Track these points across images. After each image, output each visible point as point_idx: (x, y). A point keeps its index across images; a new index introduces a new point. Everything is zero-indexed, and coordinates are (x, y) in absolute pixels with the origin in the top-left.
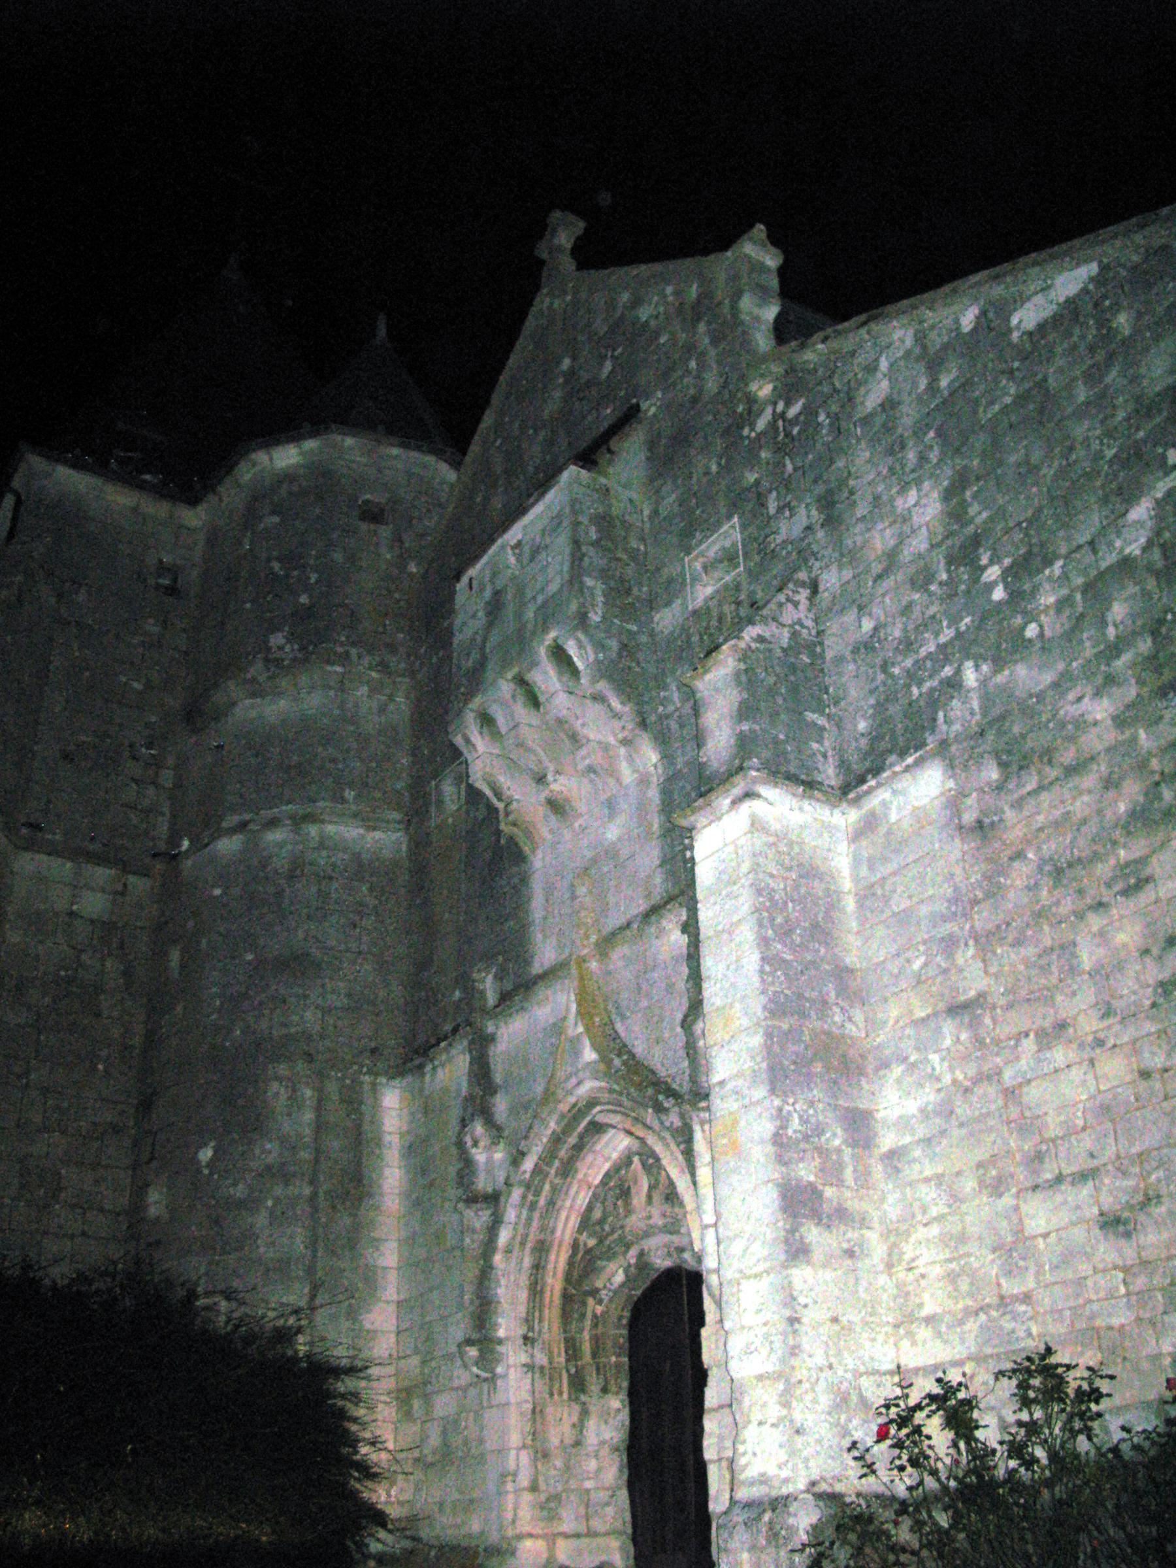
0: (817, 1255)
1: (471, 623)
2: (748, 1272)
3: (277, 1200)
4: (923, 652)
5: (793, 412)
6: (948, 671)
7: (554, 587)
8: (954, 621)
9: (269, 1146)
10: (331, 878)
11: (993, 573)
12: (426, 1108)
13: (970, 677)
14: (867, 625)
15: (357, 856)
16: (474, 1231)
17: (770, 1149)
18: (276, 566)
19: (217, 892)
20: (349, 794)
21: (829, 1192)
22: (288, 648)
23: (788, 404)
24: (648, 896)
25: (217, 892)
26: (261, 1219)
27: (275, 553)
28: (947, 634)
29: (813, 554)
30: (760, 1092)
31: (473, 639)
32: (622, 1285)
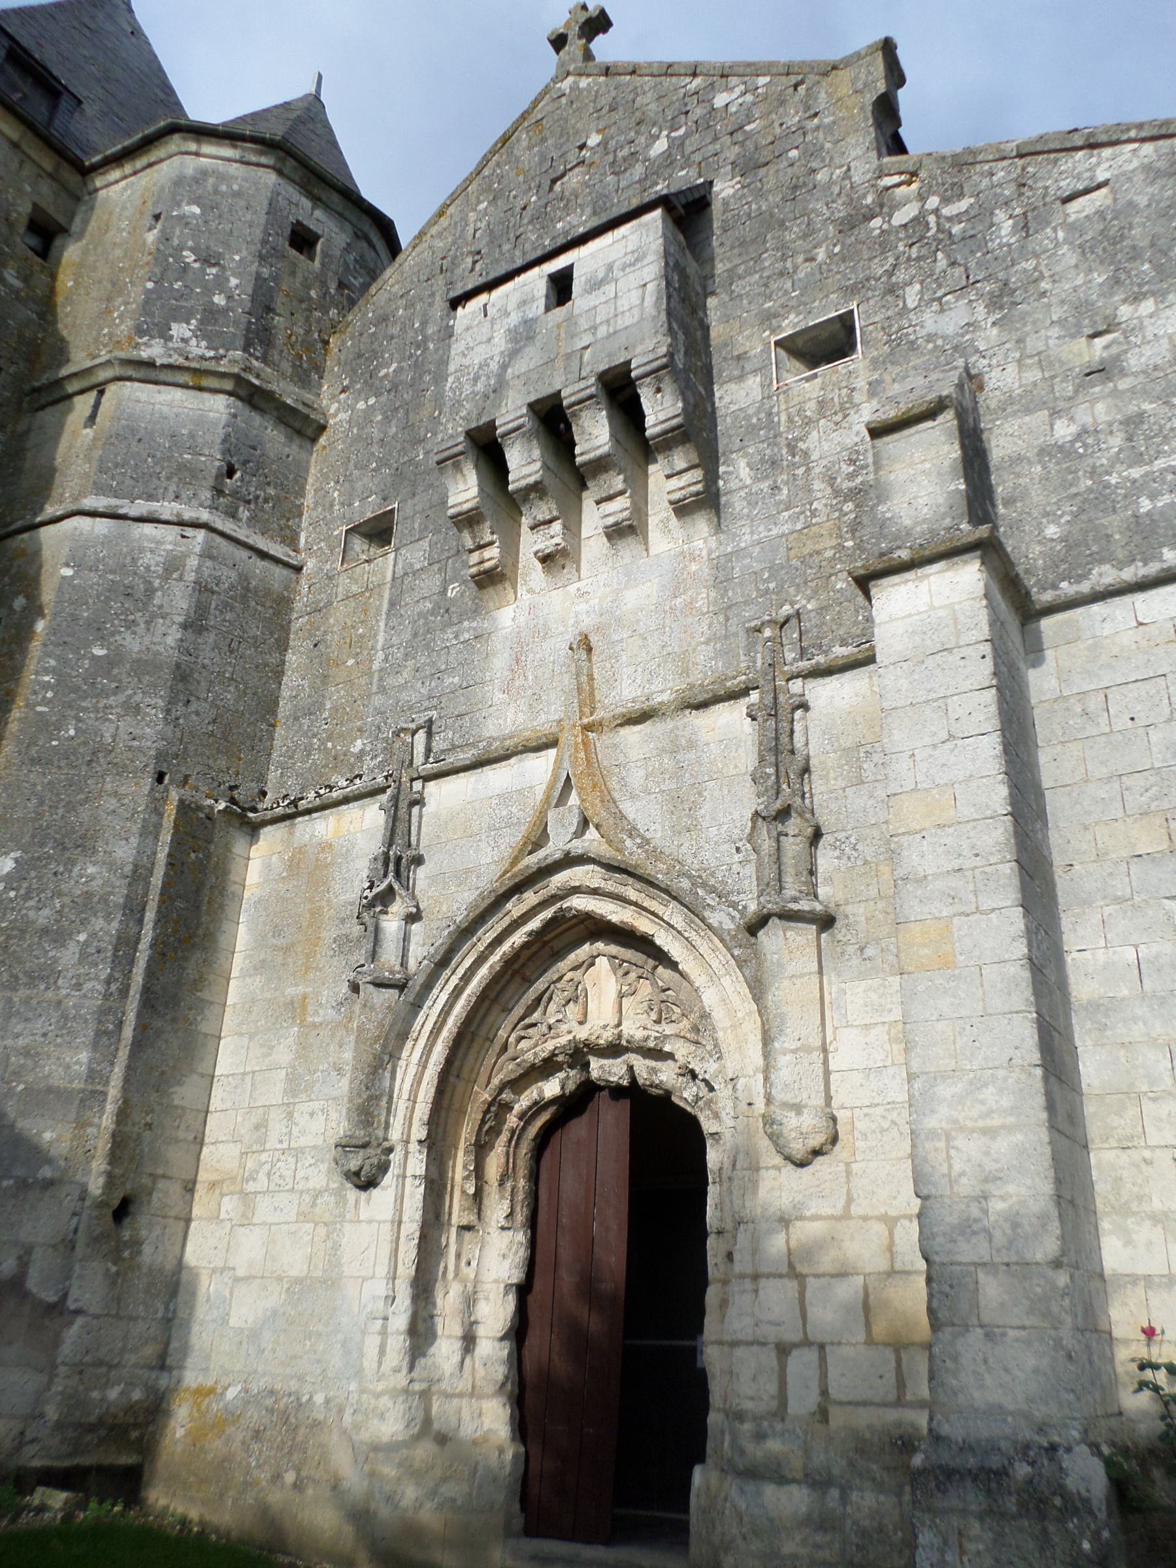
1: (481, 349)
2: (969, 1124)
3: (93, 935)
4: (1160, 464)
5: (946, 211)
7: (628, 320)
9: (91, 870)
10: (213, 592)
15: (244, 578)
16: (372, 1008)
19: (68, 572)
20: (244, 513)
22: (194, 342)
23: (946, 201)
24: (686, 672)
25: (68, 572)
26: (68, 956)
27: (190, 243)
29: (977, 351)
31: (484, 365)
32: (554, 1101)
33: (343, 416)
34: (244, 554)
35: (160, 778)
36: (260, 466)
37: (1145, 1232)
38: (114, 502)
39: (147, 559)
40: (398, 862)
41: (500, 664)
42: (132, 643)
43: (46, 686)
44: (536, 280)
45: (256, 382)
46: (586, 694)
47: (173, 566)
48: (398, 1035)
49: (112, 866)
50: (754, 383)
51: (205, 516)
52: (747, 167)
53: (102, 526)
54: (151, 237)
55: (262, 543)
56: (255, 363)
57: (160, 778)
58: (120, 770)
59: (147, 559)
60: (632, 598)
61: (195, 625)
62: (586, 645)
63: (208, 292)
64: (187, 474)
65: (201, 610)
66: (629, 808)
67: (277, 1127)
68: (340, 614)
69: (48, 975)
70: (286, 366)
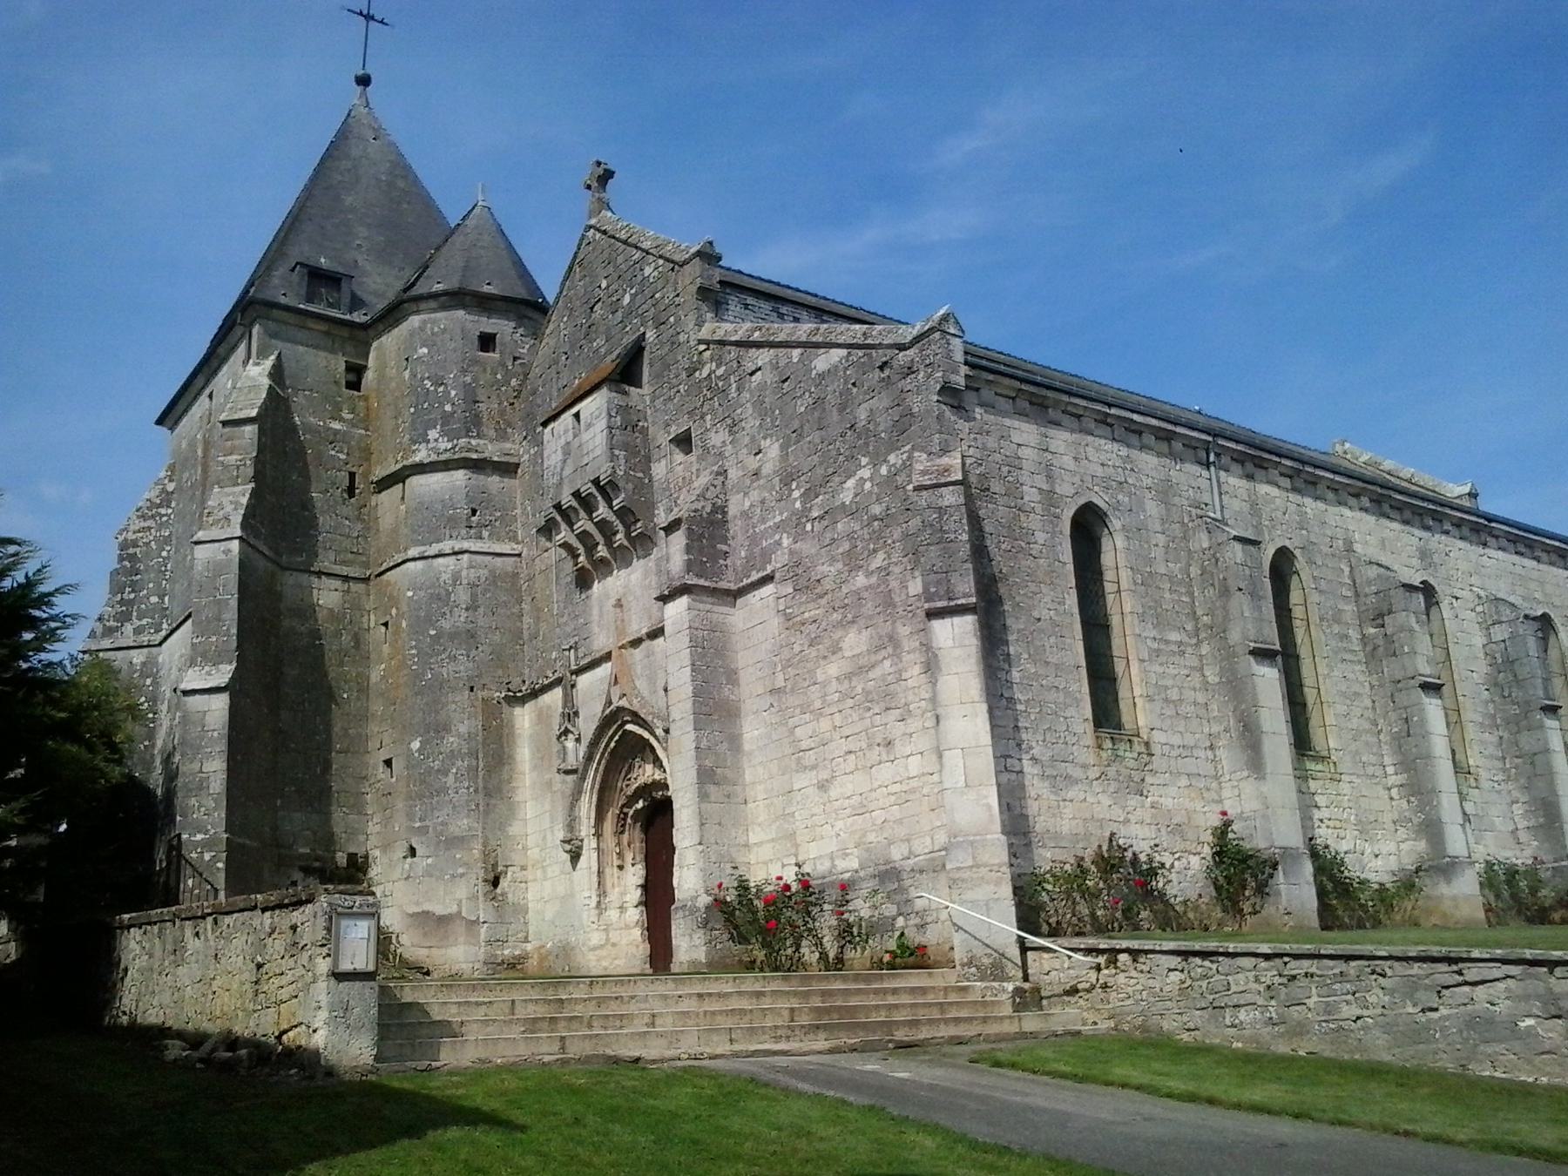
0: (712, 799)
6: (777, 537)
7: (598, 452)
8: (781, 514)
11: (796, 494)
12: (542, 718)
13: (785, 542)
14: (747, 504)
17: (693, 753)
18: (428, 383)
19: (410, 594)
20: (485, 534)
21: (719, 771)
23: (718, 367)
25: (410, 594)
26: (450, 780)
28: (778, 519)
30: (691, 728)
33: (526, 457)
34: (489, 558)
35: (472, 689)
36: (489, 501)
37: (758, 829)
38: (422, 548)
39: (444, 577)
40: (571, 714)
41: (595, 612)
42: (446, 624)
43: (413, 656)
44: (567, 417)
45: (475, 456)
46: (620, 631)
47: (456, 578)
48: (577, 794)
49: (459, 736)
50: (663, 462)
51: (466, 545)
52: (659, 324)
53: (420, 564)
54: (407, 374)
55: (498, 548)
56: (474, 442)
57: (472, 689)
58: (454, 690)
59: (444, 577)
60: (633, 577)
61: (472, 607)
62: (619, 604)
63: (442, 405)
64: (452, 522)
65: (474, 597)
66: (637, 683)
67: (549, 837)
68: (539, 579)
69: (444, 790)
70: (492, 433)
